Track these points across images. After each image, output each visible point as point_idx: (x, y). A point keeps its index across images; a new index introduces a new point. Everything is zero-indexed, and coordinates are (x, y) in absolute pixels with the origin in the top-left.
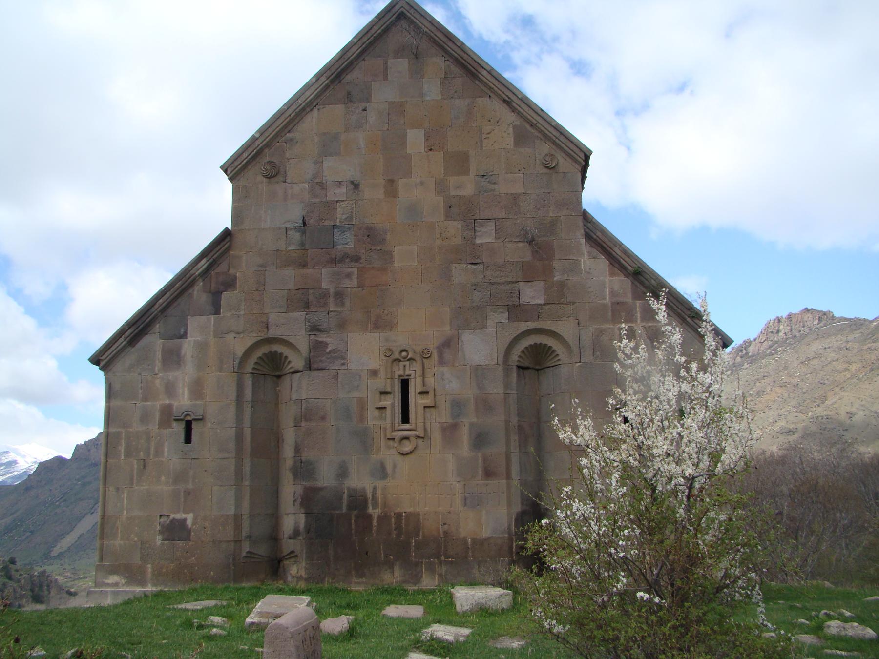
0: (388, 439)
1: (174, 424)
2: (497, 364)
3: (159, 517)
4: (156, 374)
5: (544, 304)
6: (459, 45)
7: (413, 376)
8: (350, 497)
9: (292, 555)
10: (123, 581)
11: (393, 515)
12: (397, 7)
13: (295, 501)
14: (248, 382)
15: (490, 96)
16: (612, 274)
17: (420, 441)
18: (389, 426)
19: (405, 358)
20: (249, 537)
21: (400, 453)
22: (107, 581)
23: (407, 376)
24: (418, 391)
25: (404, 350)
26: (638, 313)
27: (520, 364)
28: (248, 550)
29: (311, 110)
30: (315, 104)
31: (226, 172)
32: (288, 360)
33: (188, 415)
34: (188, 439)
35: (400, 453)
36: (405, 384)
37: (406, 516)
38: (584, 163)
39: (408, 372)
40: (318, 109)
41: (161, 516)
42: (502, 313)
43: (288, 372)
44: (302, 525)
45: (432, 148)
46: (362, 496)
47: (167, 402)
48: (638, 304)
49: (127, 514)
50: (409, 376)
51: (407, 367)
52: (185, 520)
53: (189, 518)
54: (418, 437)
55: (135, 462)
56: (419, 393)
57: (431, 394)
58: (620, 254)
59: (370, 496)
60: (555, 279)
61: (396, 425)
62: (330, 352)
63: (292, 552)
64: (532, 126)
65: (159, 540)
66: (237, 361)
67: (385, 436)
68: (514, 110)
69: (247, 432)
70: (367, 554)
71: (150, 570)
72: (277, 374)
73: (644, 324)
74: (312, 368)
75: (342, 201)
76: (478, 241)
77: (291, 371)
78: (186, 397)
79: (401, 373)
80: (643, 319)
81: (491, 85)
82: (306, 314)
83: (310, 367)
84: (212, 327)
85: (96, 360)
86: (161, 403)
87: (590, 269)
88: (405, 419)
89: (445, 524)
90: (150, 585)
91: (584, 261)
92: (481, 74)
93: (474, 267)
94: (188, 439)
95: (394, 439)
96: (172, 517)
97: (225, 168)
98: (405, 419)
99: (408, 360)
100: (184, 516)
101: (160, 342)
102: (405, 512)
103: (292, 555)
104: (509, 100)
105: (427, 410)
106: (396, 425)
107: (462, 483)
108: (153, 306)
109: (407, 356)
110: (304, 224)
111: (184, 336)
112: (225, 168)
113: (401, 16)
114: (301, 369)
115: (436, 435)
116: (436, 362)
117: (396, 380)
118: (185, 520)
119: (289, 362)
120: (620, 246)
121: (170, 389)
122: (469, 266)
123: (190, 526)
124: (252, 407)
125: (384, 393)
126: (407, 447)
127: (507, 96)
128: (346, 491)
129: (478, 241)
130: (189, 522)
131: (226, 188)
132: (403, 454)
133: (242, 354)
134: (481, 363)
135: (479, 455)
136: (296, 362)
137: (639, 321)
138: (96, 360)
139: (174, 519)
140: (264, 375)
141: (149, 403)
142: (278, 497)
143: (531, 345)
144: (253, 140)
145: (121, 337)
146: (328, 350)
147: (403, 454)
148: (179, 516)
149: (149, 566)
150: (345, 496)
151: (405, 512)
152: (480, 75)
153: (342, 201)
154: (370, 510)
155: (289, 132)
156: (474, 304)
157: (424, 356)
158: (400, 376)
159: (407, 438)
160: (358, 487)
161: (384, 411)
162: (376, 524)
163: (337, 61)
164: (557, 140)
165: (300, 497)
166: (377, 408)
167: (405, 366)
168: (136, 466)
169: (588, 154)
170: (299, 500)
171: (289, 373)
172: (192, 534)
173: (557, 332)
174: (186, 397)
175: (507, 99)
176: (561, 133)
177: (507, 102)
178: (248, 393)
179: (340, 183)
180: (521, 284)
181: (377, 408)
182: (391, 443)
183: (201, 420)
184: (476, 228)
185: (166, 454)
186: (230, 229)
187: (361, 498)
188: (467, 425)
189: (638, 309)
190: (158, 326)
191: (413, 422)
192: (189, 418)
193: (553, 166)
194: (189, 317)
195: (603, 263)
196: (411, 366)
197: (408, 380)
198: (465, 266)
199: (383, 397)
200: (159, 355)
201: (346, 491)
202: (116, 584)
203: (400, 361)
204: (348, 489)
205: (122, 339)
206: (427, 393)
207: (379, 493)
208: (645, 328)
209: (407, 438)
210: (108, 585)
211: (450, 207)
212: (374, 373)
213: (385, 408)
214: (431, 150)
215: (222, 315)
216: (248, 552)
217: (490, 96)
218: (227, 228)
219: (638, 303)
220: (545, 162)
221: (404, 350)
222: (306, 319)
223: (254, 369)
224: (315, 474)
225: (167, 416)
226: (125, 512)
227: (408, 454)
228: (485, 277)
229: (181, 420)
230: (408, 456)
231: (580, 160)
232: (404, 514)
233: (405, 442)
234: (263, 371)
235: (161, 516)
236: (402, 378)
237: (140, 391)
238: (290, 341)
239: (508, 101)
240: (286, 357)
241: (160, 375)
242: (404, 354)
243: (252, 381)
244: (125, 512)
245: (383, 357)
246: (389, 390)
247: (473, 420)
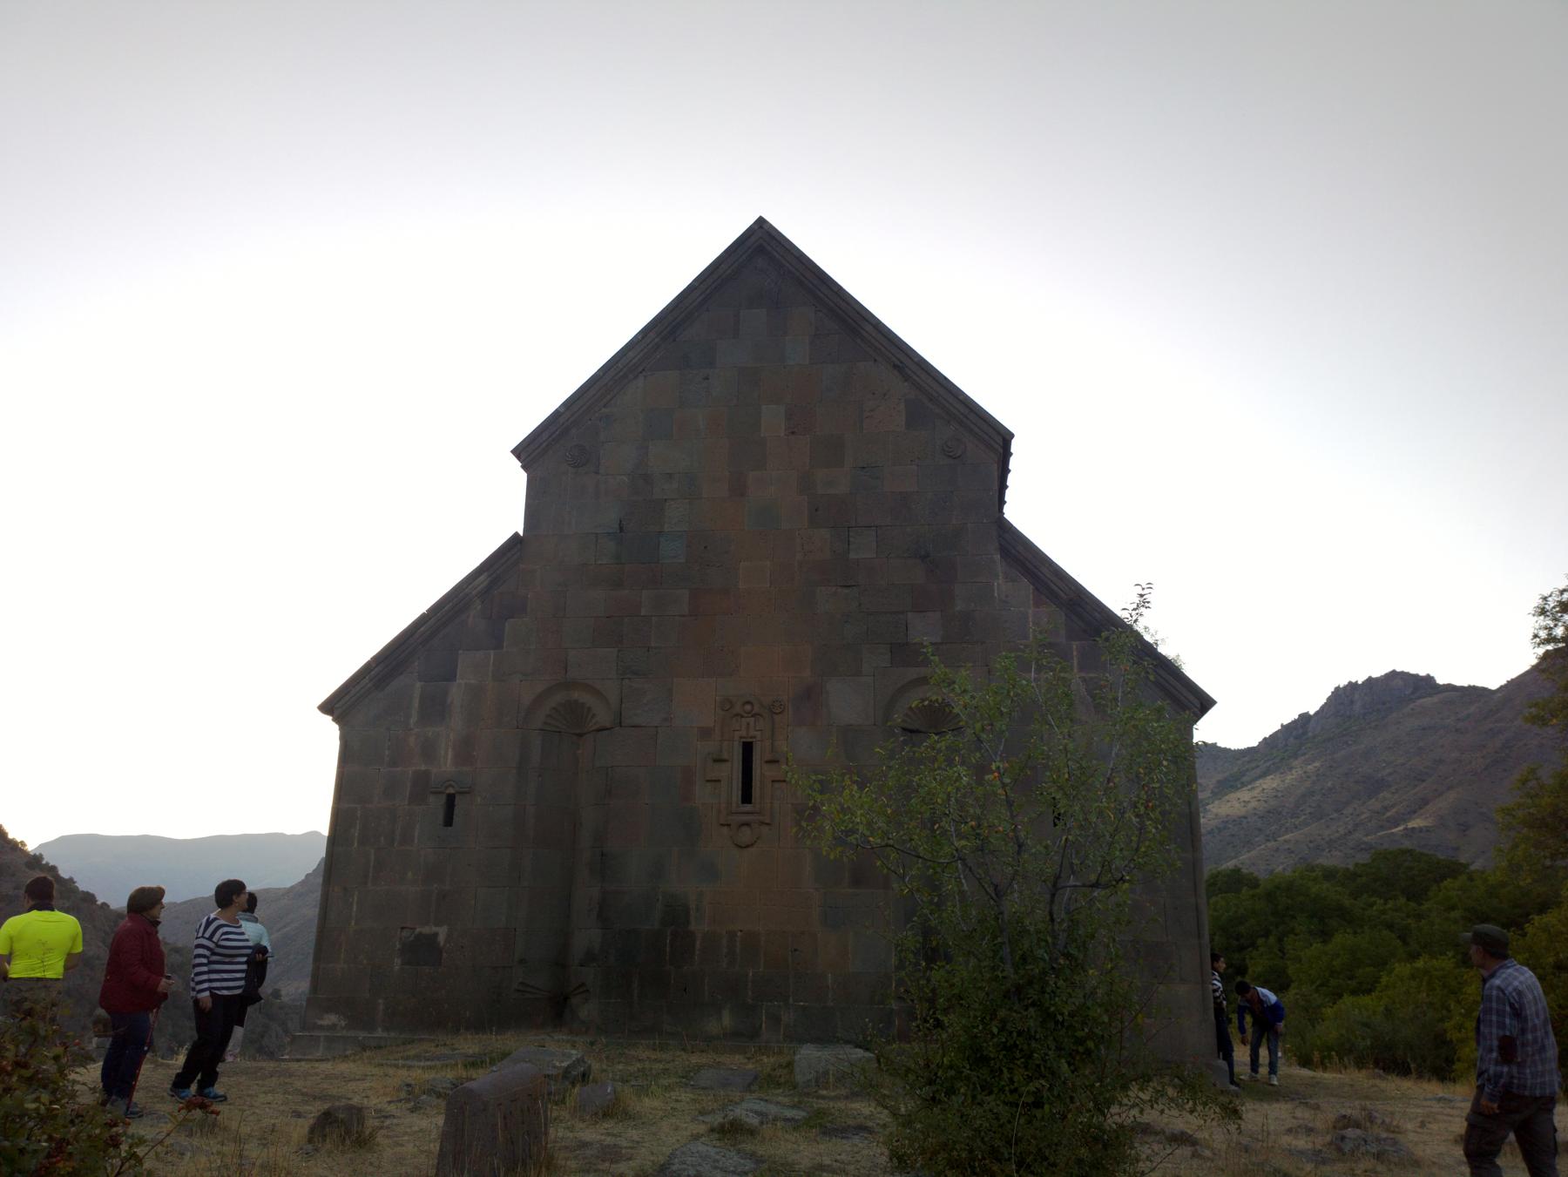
0: (722, 825)
1: (432, 799)
3: (399, 930)
4: (411, 729)
5: (941, 643)
6: (836, 290)
9: (581, 990)
10: (343, 1023)
12: (753, 239)
15: (875, 360)
16: (1037, 604)
19: (749, 713)
20: (522, 961)
22: (320, 1022)
23: (751, 738)
24: (766, 759)
25: (748, 703)
26: (1075, 659)
27: (905, 725)
28: (521, 980)
29: (636, 377)
30: (640, 369)
31: (518, 457)
33: (450, 786)
34: (449, 821)
36: (748, 748)
38: (1001, 451)
39: (752, 733)
40: (645, 377)
41: (403, 928)
43: (591, 729)
45: (796, 430)
47: (423, 768)
48: (1074, 647)
49: (355, 924)
50: (755, 737)
51: (752, 724)
52: (436, 935)
53: (442, 932)
54: (763, 823)
55: (373, 851)
56: (767, 762)
58: (1048, 576)
60: (958, 608)
61: (734, 805)
63: (583, 985)
64: (931, 400)
65: (398, 961)
68: (907, 378)
70: (685, 990)
71: (381, 1007)
72: (578, 731)
73: (1083, 675)
74: (623, 724)
75: (673, 499)
76: (852, 556)
77: (593, 728)
78: (449, 761)
79: (744, 733)
80: (1081, 669)
81: (877, 344)
82: (619, 651)
83: (620, 723)
85: (328, 707)
86: (414, 768)
87: (1007, 596)
88: (747, 797)
89: (796, 950)
90: (380, 1029)
91: (998, 584)
92: (864, 330)
93: (846, 591)
94: (449, 821)
95: (729, 825)
96: (418, 930)
97: (518, 452)
98: (747, 797)
99: (752, 716)
100: (435, 929)
101: (418, 685)
102: (741, 931)
103: (581, 990)
104: (901, 365)
106: (734, 805)
108: (412, 636)
110: (621, 529)
111: (451, 677)
112: (518, 452)
113: (760, 250)
114: (608, 725)
117: (736, 744)
118: (436, 935)
119: (594, 715)
120: (1050, 565)
121: (429, 751)
122: (840, 590)
123: (442, 944)
124: (540, 776)
126: (746, 835)
127: (899, 359)
128: (660, 898)
129: (852, 556)
130: (441, 939)
131: (516, 479)
132: (741, 847)
136: (603, 717)
137: (1075, 670)
138: (328, 707)
139: (420, 933)
140: (560, 732)
141: (398, 769)
144: (556, 415)
145: (365, 678)
147: (741, 847)
148: (426, 930)
149: (380, 1001)
151: (741, 931)
152: (862, 331)
153: (673, 499)
154: (692, 927)
155: (604, 406)
158: (741, 737)
159: (748, 824)
163: (671, 311)
164: (965, 419)
166: (708, 781)
167: (748, 724)
168: (372, 857)
169: (1007, 437)
171: (593, 731)
172: (444, 955)
174: (449, 761)
175: (899, 363)
176: (971, 410)
177: (899, 368)
179: (670, 475)
180: (910, 615)
181: (708, 781)
182: (725, 829)
183: (469, 793)
184: (851, 539)
185: (416, 841)
186: (521, 534)
189: (1075, 653)
190: (416, 664)
192: (451, 791)
193: (958, 455)
194: (460, 652)
195: (1025, 588)
197: (752, 743)
198: (834, 589)
200: (416, 703)
201: (660, 898)
202: (333, 1027)
203: (742, 717)
205: (366, 680)
206: (778, 761)
208: (1084, 680)
209: (748, 824)
210: (321, 1028)
211: (816, 510)
212: (705, 733)
213: (719, 781)
214: (793, 433)
215: (505, 649)
216: (521, 983)
217: (875, 360)
218: (516, 534)
219: (1075, 645)
220: (947, 449)
221: (748, 703)
222: (618, 656)
223: (545, 723)
225: (422, 787)
226: (353, 923)
228: (860, 605)
229: (440, 793)
230: (749, 849)
231: (996, 446)
232: (739, 934)
233: (744, 829)
235: (403, 928)
236: (744, 740)
237: (387, 753)
239: (899, 367)
240: (589, 709)
241: (416, 730)
242: (748, 707)
244: (353, 923)
246: (725, 756)
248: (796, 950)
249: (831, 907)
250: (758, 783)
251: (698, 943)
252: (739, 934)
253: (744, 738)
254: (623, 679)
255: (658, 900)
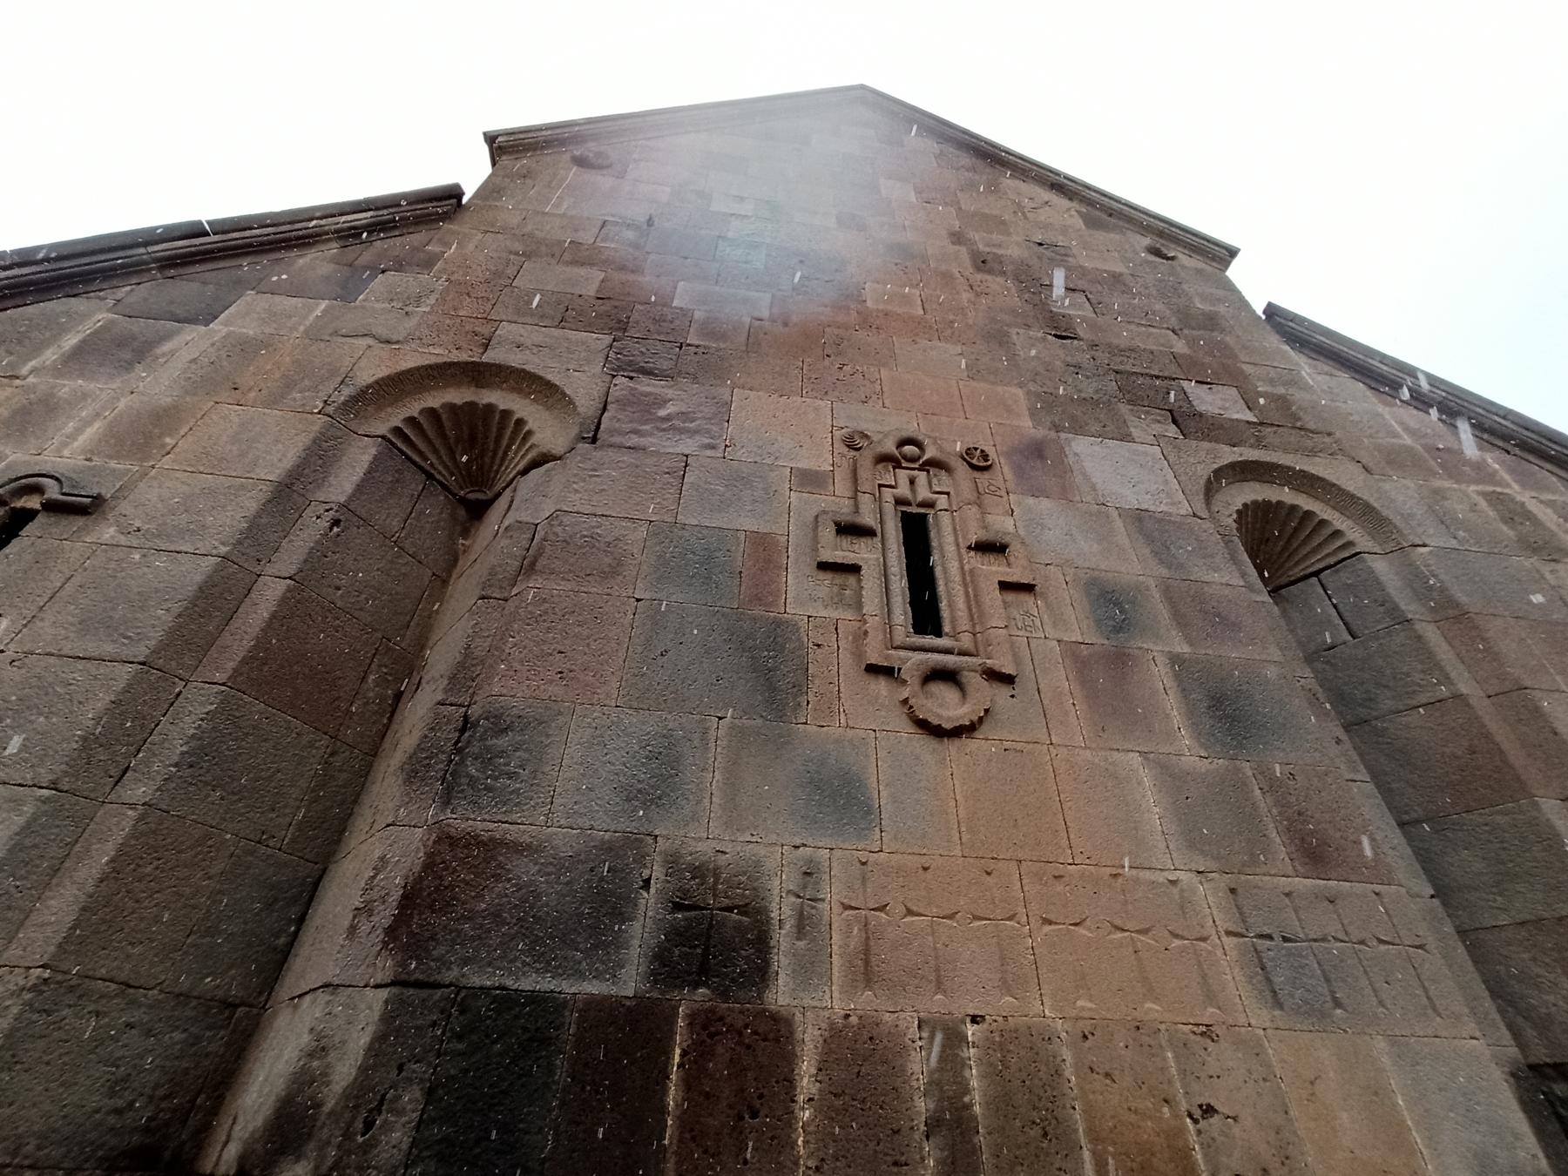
0: (872, 669)
2: (1195, 515)
7: (942, 501)
8: (678, 907)
11: (913, 1031)
13: (365, 910)
14: (359, 458)
17: (1002, 692)
18: (873, 623)
19: (913, 460)
21: (924, 726)
23: (921, 505)
24: (973, 540)
32: (527, 428)
35: (924, 726)
36: (916, 532)
37: (988, 1046)
39: (923, 493)
42: (1159, 422)
44: (344, 1071)
46: (743, 910)
50: (930, 505)
54: (994, 676)
57: (1015, 549)
59: (781, 909)
62: (668, 418)
66: (347, 392)
67: (858, 654)
69: (270, 593)
79: (903, 490)
82: (614, 341)
84: (311, 318)
88: (926, 616)
89: (1209, 1110)
98: (926, 616)
102: (975, 1020)
105: (1011, 597)
107: (1224, 881)
109: (919, 458)
114: (558, 449)
115: (1058, 678)
116: (1011, 485)
119: (529, 433)
124: (336, 523)
125: (850, 530)
126: (947, 706)
133: (371, 380)
134: (1144, 506)
135: (1247, 769)
136: (547, 431)
140: (430, 476)
142: (301, 920)
143: (1255, 503)
146: (662, 413)
150: (650, 904)
151: (975, 1020)
154: (782, 994)
156: (1083, 395)
157: (974, 461)
160: (722, 859)
161: (851, 580)
162: (814, 1089)
165: (396, 895)
166: (823, 566)
170: (385, 915)
173: (1320, 475)
178: (342, 483)
181: (823, 566)
182: (881, 686)
187: (734, 916)
188: (1160, 659)
191: (964, 624)
196: (935, 481)
197: (925, 515)
199: (845, 541)
201: (657, 872)
203: (898, 465)
204: (673, 861)
207: (833, 893)
212: (810, 480)
213: (854, 569)
223: (397, 431)
224: (511, 776)
227: (958, 732)
232: (971, 1030)
234: (426, 459)
238: (549, 377)
242: (908, 449)
243: (375, 458)
245: (841, 448)
246: (868, 519)
247: (1178, 649)
248: (1209, 1110)
249: (1269, 937)
250: (958, 590)
251: (806, 1068)
252: (971, 1030)
253: (909, 504)
254: (614, 376)
255: (647, 884)
